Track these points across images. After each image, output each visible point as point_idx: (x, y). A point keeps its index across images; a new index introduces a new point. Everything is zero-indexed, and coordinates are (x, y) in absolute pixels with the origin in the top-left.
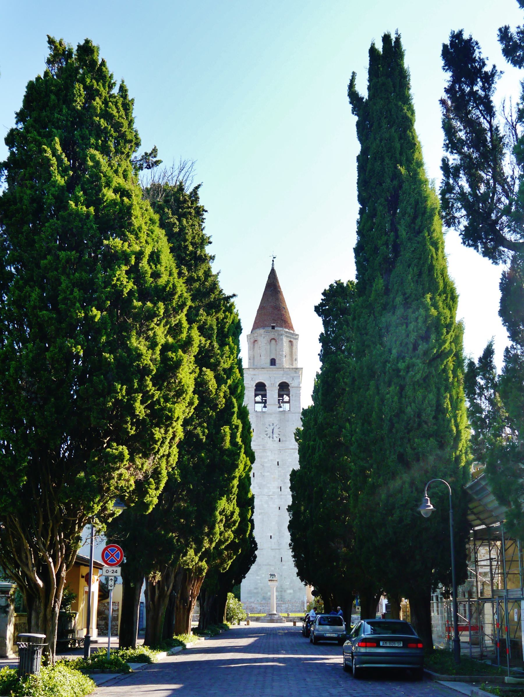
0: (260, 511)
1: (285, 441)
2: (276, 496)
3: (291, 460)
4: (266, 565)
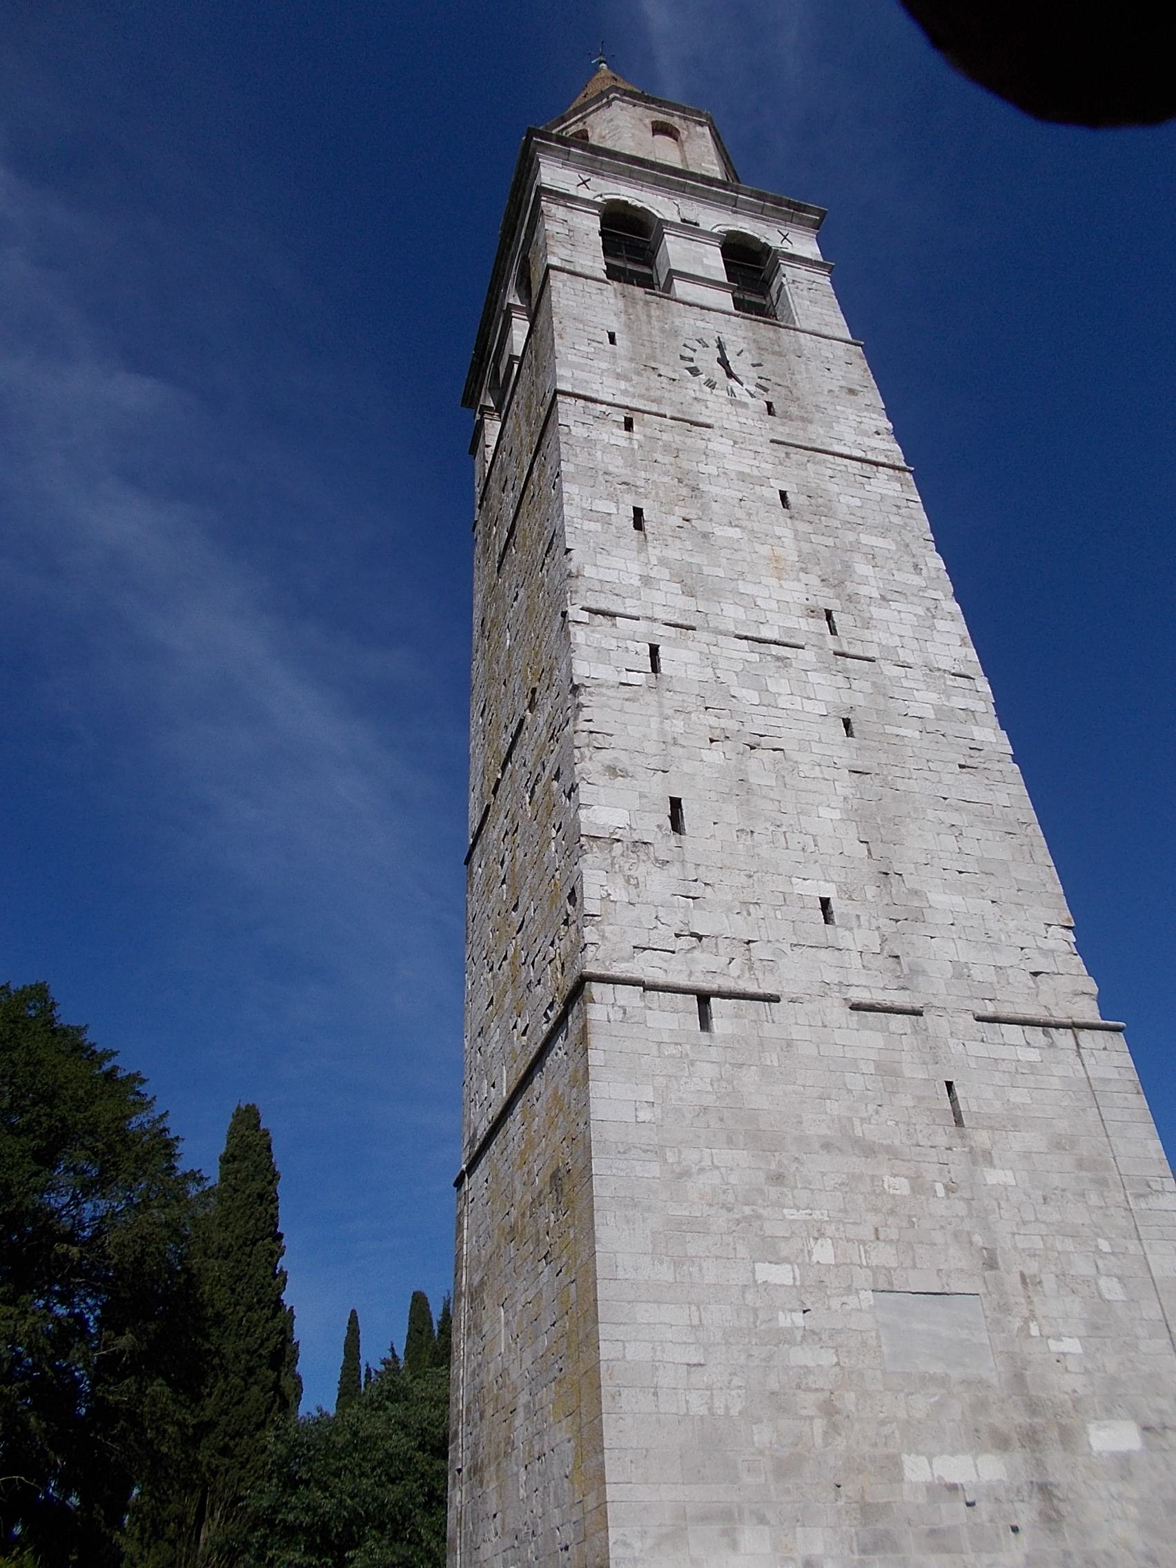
0: (713, 721)
4: (827, 1146)
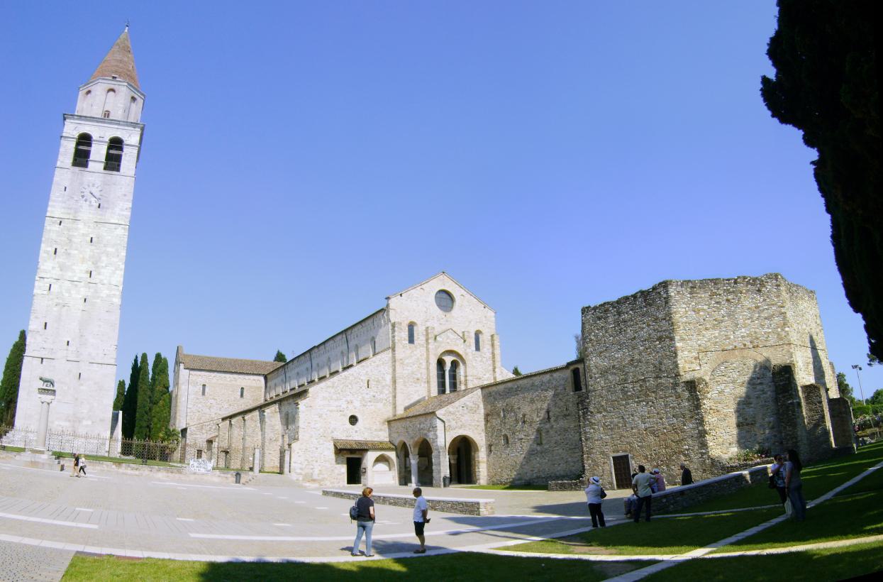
0: (57, 301)
1: (107, 208)
2: (82, 284)
3: (110, 238)
